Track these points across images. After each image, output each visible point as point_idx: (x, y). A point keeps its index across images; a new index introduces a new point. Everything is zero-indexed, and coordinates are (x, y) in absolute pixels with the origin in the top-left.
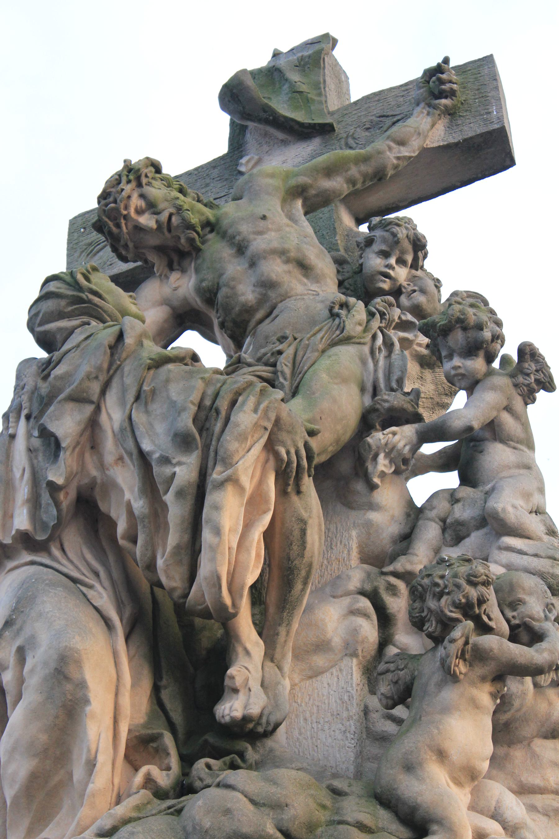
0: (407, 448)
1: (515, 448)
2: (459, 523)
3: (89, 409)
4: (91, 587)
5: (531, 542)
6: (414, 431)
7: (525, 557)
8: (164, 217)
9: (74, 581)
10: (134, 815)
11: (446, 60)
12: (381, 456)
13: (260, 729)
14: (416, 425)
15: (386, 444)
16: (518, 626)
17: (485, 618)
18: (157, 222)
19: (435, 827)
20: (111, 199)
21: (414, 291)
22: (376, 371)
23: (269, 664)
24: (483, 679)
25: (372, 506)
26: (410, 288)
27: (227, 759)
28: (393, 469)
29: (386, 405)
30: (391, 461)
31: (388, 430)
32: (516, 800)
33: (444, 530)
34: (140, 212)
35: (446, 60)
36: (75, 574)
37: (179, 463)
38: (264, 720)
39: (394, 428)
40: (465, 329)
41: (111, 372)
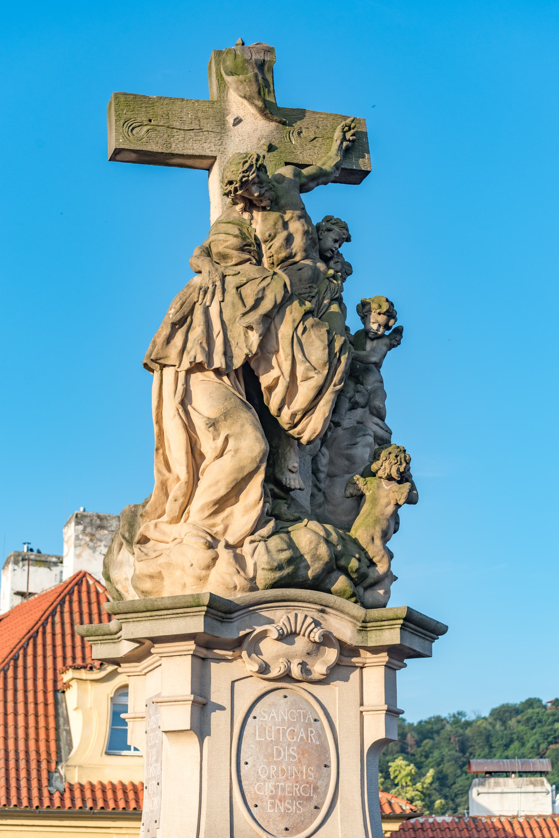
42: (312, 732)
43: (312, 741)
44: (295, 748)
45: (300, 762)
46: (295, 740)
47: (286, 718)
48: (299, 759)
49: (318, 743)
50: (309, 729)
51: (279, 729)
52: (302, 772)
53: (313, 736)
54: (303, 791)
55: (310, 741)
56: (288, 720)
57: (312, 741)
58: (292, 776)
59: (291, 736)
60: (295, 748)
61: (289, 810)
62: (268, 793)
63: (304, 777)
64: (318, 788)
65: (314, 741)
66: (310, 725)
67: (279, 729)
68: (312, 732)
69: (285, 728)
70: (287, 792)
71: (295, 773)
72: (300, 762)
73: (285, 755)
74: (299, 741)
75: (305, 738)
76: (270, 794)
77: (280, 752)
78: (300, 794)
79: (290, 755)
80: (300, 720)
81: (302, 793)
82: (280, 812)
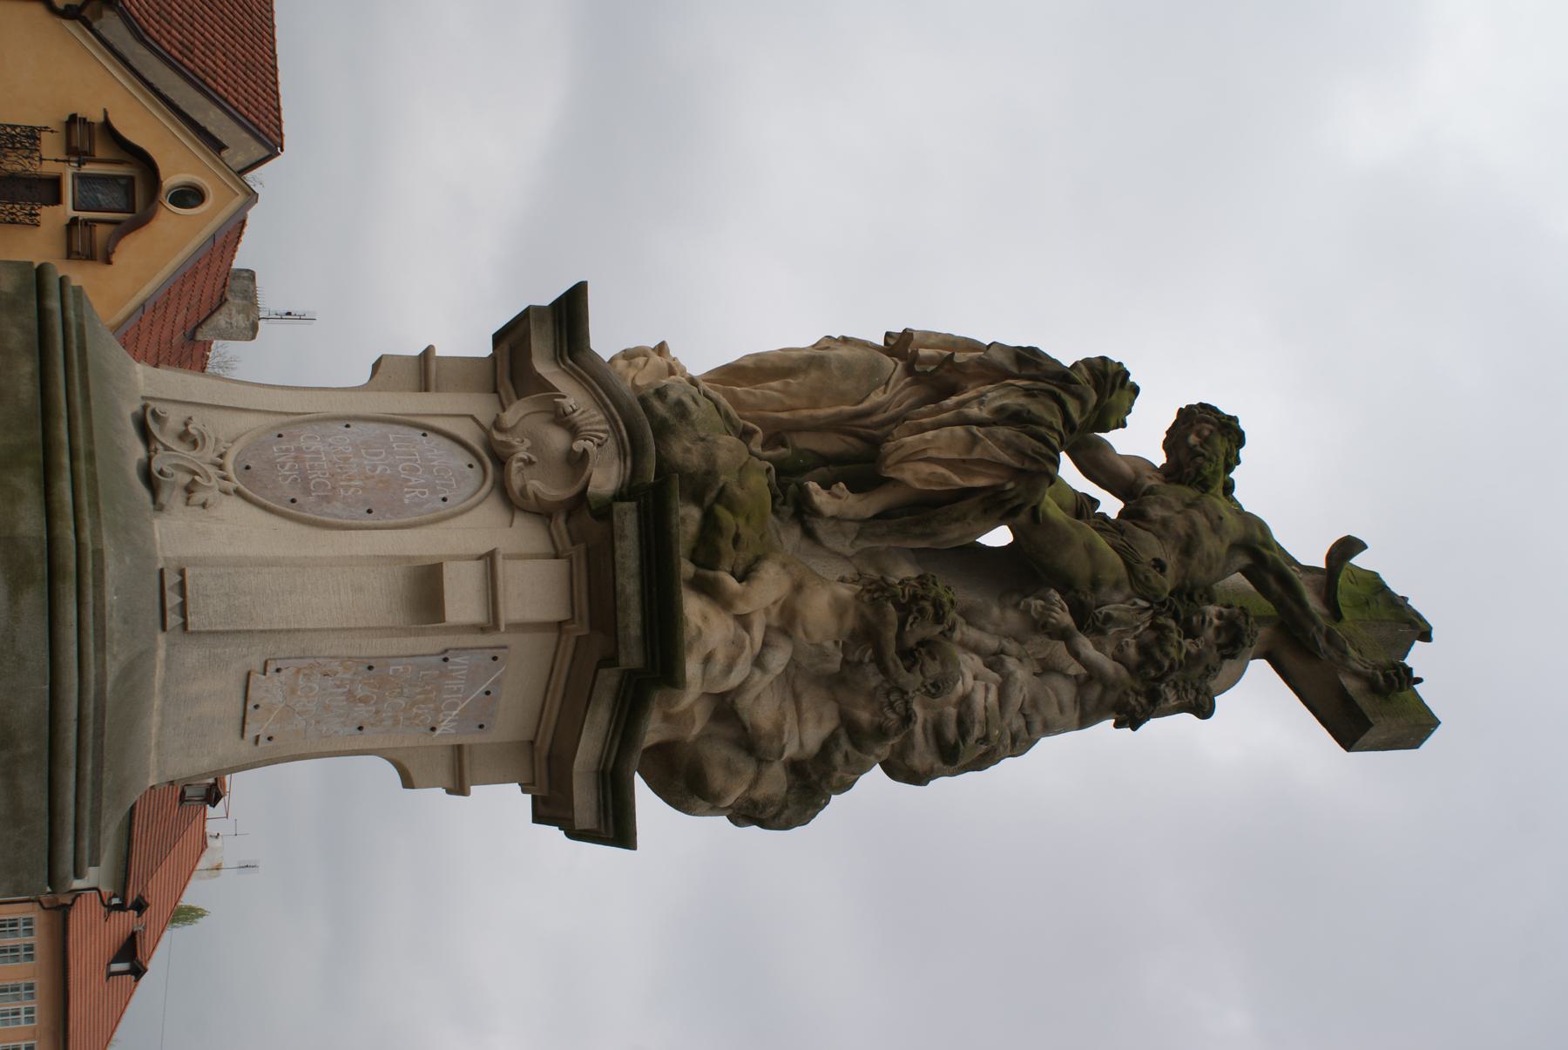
0: (1053, 621)
1: (1075, 702)
2: (1002, 663)
3: (1014, 370)
4: (885, 392)
5: (998, 713)
6: (1068, 623)
7: (983, 701)
8: (1199, 449)
9: (887, 383)
10: (722, 408)
11: (1419, 680)
12: (1042, 602)
13: (806, 517)
14: (1073, 624)
15: (1053, 604)
16: (914, 657)
17: (910, 619)
18: (1195, 446)
19: (744, 584)
20: (1201, 410)
21: (1198, 646)
22: (1114, 603)
23: (856, 526)
24: (862, 616)
25: (1003, 608)
26: (1199, 643)
27: (779, 492)
28: (1036, 617)
29: (1083, 598)
30: (1041, 614)
31: (1063, 602)
32: (782, 665)
33: (995, 654)
34: (1199, 434)
35: (1419, 680)
36: (892, 382)
37: (980, 409)
38: (813, 519)
39: (1066, 607)
40: (1157, 638)
41: (1046, 380)
42: (424, 493)
43: (407, 493)
44: (389, 472)
45: (367, 478)
46: (402, 472)
47: (435, 463)
48: (373, 477)
49: (406, 501)
50: (426, 490)
51: (415, 455)
52: (350, 480)
53: (416, 496)
54: (317, 483)
55: (406, 490)
56: (434, 466)
57: (407, 493)
58: (341, 468)
59: (407, 468)
60: (389, 472)
61: (282, 467)
62: (303, 445)
63: (342, 483)
64: (328, 502)
65: (408, 496)
66: (434, 491)
67: (415, 455)
68: (424, 493)
69: (419, 462)
70: (311, 463)
71: (346, 473)
72: (367, 478)
73: (373, 461)
74: (403, 476)
75: (410, 484)
76: (304, 448)
77: (377, 456)
78: (311, 480)
79: (374, 468)
80: (439, 479)
81: (313, 482)
82: (276, 459)
